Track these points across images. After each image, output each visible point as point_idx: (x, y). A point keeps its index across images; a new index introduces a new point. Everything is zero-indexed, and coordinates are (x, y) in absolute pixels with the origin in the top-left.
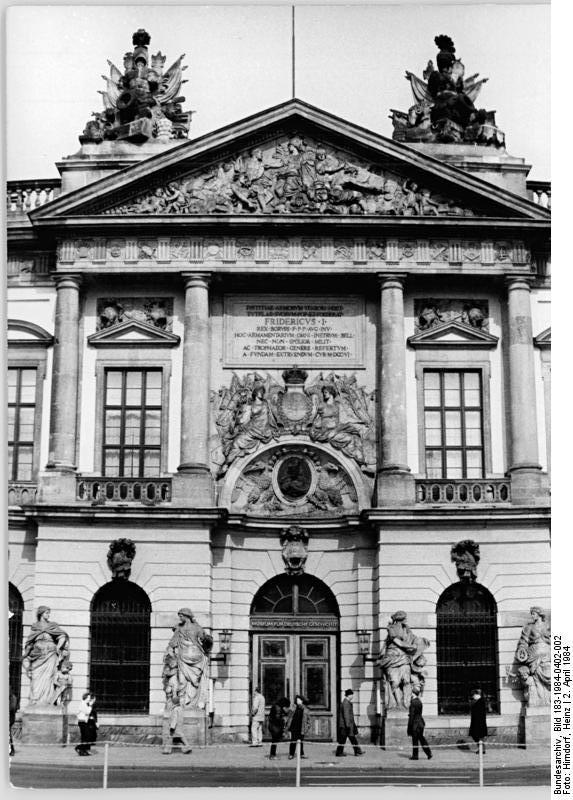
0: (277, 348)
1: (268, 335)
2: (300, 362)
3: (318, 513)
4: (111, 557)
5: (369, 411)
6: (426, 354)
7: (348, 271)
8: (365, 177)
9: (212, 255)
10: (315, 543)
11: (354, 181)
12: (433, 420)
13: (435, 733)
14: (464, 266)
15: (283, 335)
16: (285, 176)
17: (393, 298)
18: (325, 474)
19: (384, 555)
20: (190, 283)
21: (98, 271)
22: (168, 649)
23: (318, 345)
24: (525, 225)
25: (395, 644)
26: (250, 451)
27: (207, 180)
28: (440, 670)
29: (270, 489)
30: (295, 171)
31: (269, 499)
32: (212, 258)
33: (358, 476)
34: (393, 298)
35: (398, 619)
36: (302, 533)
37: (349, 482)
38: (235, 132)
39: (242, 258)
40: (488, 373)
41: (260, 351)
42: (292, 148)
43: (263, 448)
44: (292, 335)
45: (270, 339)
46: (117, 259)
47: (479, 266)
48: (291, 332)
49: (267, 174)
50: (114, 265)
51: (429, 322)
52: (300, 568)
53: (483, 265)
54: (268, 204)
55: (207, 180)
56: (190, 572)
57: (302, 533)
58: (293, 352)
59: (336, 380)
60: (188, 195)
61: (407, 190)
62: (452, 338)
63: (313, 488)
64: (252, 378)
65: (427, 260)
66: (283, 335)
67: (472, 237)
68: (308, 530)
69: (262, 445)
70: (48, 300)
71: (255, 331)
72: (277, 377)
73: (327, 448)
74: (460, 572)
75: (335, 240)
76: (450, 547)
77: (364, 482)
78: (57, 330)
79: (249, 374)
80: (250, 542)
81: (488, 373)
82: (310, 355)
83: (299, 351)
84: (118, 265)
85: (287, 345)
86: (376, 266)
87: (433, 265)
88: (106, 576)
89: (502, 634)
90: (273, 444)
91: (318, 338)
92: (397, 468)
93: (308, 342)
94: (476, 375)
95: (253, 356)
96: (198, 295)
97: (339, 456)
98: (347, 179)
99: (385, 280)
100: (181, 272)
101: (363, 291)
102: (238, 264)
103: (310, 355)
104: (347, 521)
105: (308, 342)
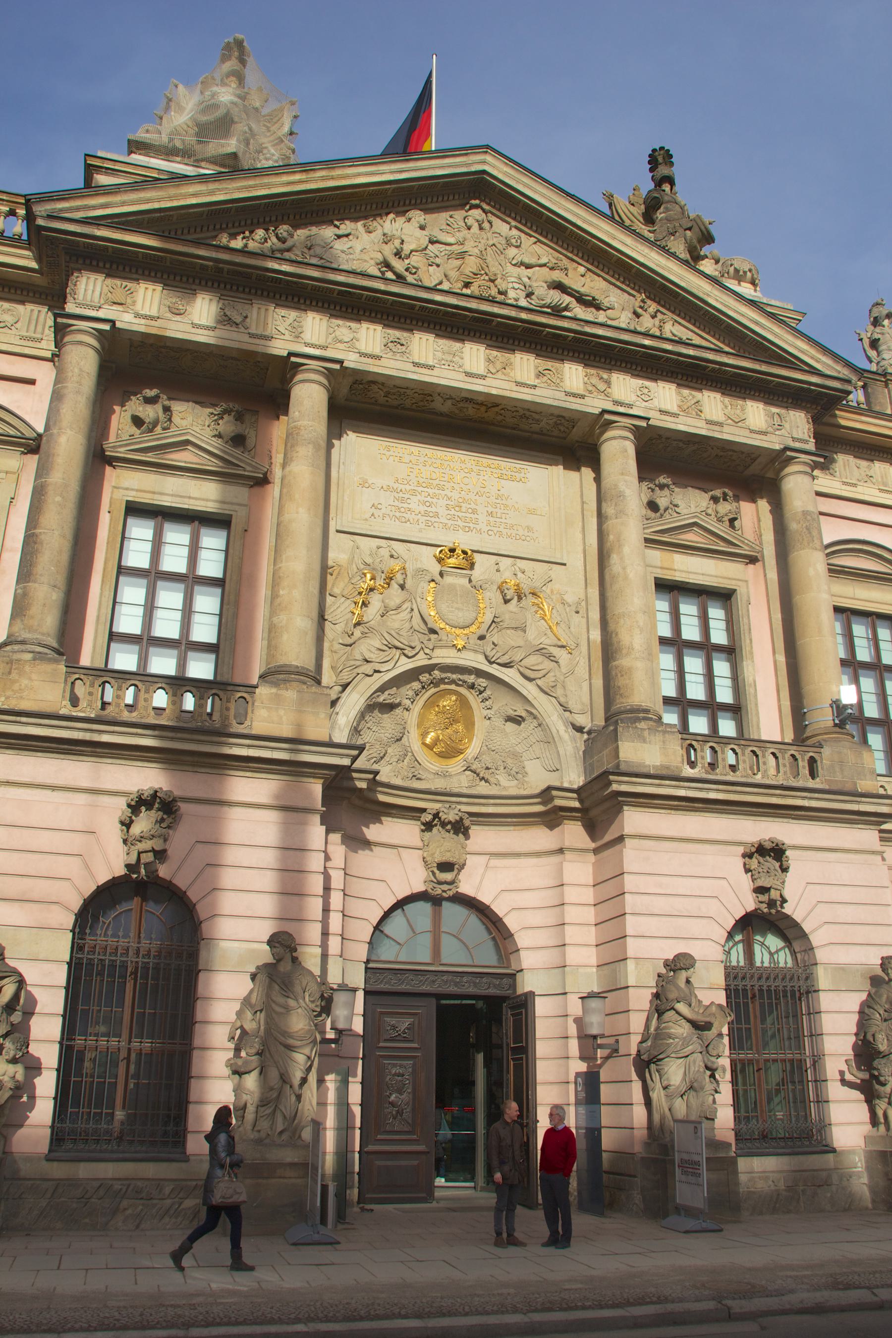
0: (426, 514)
1: (414, 493)
3: (483, 789)
4: (127, 824)
5: (572, 629)
7: (556, 403)
9: (340, 342)
10: (482, 837)
11: (566, 281)
12: (667, 660)
13: (761, 1186)
14: (726, 429)
15: (435, 496)
16: (462, 255)
17: (619, 453)
18: (498, 722)
19: (632, 855)
20: (299, 377)
21: (142, 329)
22: (239, 1014)
23: (491, 519)
25: (678, 1013)
26: (383, 668)
28: (733, 1063)
29: (405, 739)
30: (476, 251)
31: (401, 759)
32: (341, 346)
33: (562, 728)
34: (619, 453)
35: (680, 964)
37: (549, 740)
38: (392, 172)
39: (390, 355)
40: (745, 598)
41: (398, 514)
42: (470, 221)
45: (415, 499)
46: (178, 318)
47: (747, 433)
48: (447, 492)
49: (430, 247)
50: (172, 326)
51: (662, 508)
52: (452, 883)
53: (752, 431)
57: (461, 819)
58: (450, 522)
59: (520, 575)
60: (306, 250)
61: (640, 311)
62: (692, 537)
63: (473, 749)
64: (385, 553)
66: (435, 496)
68: (471, 814)
69: (404, 659)
70: (32, 382)
71: (391, 484)
72: (426, 559)
73: (510, 676)
74: (760, 890)
75: (537, 355)
76: (741, 850)
77: (574, 739)
78: (47, 428)
79: (379, 547)
81: (745, 598)
82: (480, 531)
83: (460, 523)
84: (181, 327)
85: (442, 511)
86: (594, 405)
87: (681, 419)
88: (111, 861)
89: (826, 1001)
90: (421, 661)
91: (490, 509)
92: (647, 711)
93: (474, 512)
95: (387, 520)
96: (309, 398)
97: (529, 690)
98: (557, 276)
99: (609, 424)
100: (291, 354)
101: (568, 442)
102: (383, 362)
103: (480, 531)
104: (552, 798)
105: (474, 512)
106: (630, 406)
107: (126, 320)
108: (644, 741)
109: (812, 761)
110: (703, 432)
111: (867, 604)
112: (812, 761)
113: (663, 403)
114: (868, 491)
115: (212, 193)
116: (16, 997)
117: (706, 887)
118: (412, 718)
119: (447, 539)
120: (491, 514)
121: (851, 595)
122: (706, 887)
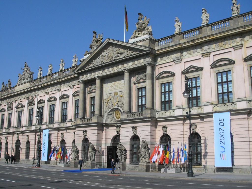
2: (117, 91)
6: (137, 85)
8: (122, 50)
24: (145, 53)
26: (108, 110)
27: (99, 58)
36: (118, 126)
43: (110, 109)
44: (116, 86)
47: (140, 64)
48: (116, 85)
54: (107, 61)
55: (99, 58)
56: (124, 135)
57: (118, 126)
65: (130, 65)
67: (138, 58)
72: (113, 95)
80: (110, 128)
86: (123, 69)
90: (111, 108)
94: (144, 88)
103: (118, 89)
106: (126, 67)
107: (83, 79)
108: (123, 115)
109: (142, 114)
110: (135, 67)
111: (164, 82)
112: (142, 114)
113: (130, 65)
114: (168, 60)
115: (85, 62)
116: (76, 149)
117: (128, 133)
118: (114, 115)
119: (114, 91)
120: (120, 86)
121: (164, 81)
122: (128, 133)
